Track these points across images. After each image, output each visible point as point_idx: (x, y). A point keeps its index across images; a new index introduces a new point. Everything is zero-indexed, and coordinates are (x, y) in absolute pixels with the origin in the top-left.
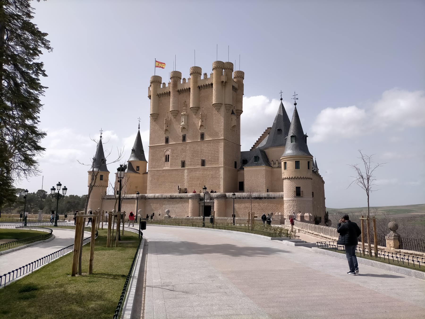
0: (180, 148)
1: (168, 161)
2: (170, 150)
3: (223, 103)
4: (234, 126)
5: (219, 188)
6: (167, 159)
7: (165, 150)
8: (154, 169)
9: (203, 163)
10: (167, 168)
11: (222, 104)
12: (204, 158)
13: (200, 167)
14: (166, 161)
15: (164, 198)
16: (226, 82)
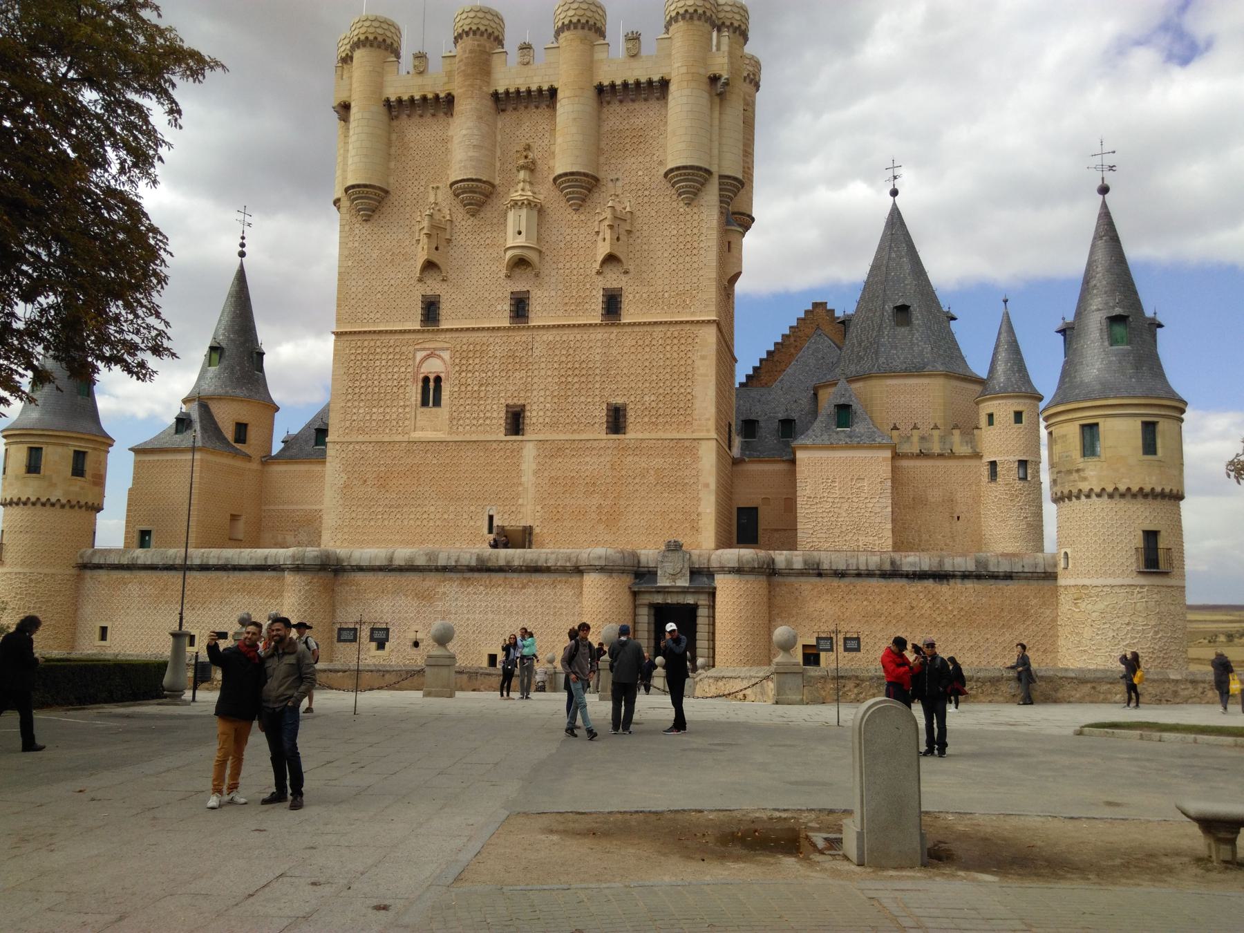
0: (498, 346)
1: (437, 403)
2: (446, 355)
3: (714, 169)
5: (695, 529)
6: (431, 391)
7: (420, 355)
8: (360, 438)
9: (616, 420)
10: (429, 435)
11: (709, 172)
12: (619, 401)
13: (604, 436)
14: (425, 403)
15: (444, 569)
16: (726, 84)
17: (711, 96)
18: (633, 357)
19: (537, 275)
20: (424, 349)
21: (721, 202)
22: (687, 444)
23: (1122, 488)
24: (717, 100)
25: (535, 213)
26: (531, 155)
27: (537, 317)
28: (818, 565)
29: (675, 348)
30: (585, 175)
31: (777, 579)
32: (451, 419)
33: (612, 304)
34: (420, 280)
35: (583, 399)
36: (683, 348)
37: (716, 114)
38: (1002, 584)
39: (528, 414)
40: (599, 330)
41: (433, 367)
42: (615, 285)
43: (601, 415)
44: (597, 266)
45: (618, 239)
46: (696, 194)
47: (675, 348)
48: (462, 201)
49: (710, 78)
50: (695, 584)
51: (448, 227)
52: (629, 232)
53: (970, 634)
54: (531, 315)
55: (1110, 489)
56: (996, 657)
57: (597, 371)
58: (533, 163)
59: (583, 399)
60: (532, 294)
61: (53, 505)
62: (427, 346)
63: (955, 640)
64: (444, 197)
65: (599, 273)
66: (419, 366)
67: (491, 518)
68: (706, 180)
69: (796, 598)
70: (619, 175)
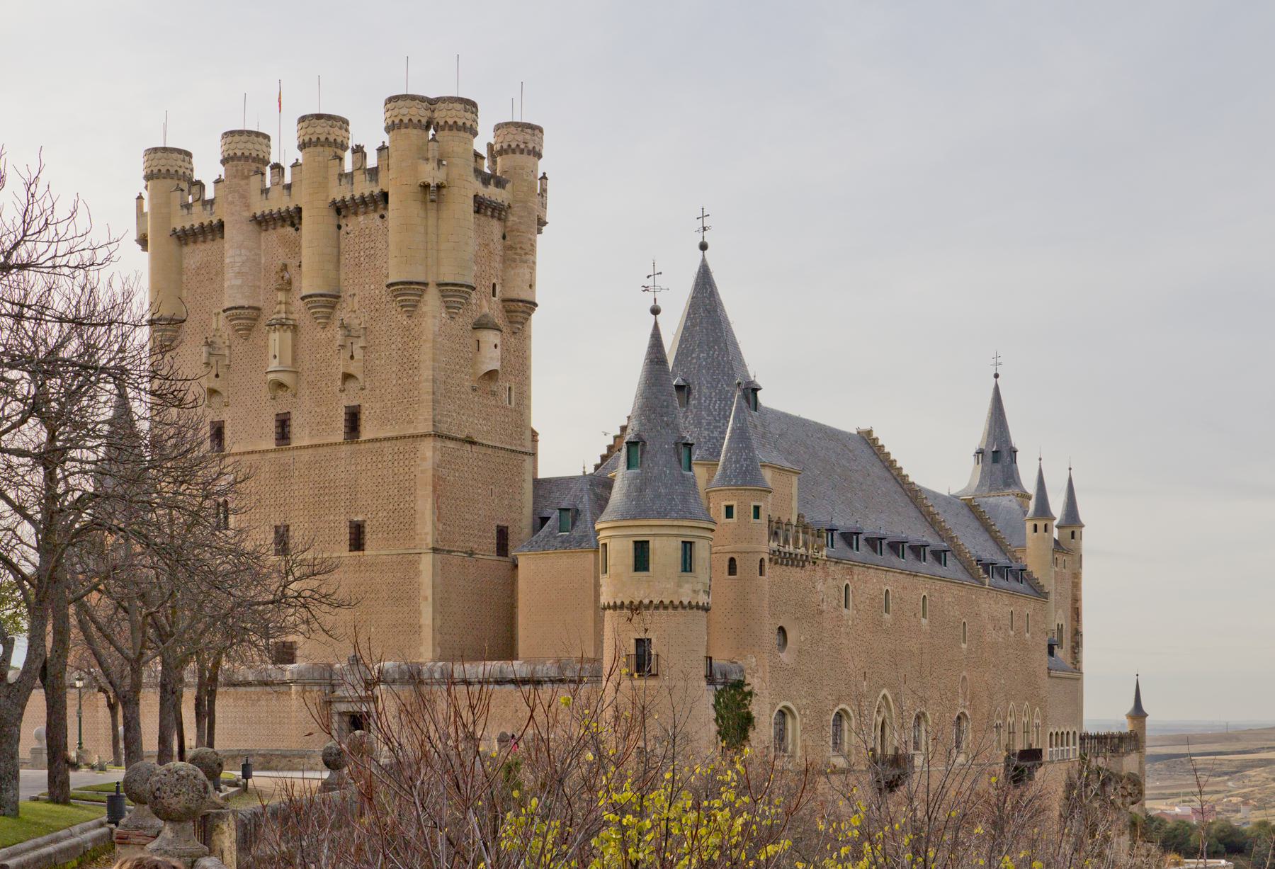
3: (430, 280)
4: (491, 375)
9: (357, 539)
11: (426, 284)
12: (359, 518)
17: (424, 202)
19: (295, 396)
22: (411, 558)
23: (619, 603)
24: (430, 205)
25: (289, 334)
26: (287, 276)
30: (321, 295)
33: (353, 420)
40: (343, 447)
42: (355, 403)
43: (345, 534)
44: (339, 383)
45: (352, 357)
46: (415, 306)
48: (234, 326)
51: (227, 352)
52: (364, 348)
54: (292, 436)
58: (289, 283)
60: (293, 415)
64: (220, 324)
65: (342, 391)
70: (356, 291)
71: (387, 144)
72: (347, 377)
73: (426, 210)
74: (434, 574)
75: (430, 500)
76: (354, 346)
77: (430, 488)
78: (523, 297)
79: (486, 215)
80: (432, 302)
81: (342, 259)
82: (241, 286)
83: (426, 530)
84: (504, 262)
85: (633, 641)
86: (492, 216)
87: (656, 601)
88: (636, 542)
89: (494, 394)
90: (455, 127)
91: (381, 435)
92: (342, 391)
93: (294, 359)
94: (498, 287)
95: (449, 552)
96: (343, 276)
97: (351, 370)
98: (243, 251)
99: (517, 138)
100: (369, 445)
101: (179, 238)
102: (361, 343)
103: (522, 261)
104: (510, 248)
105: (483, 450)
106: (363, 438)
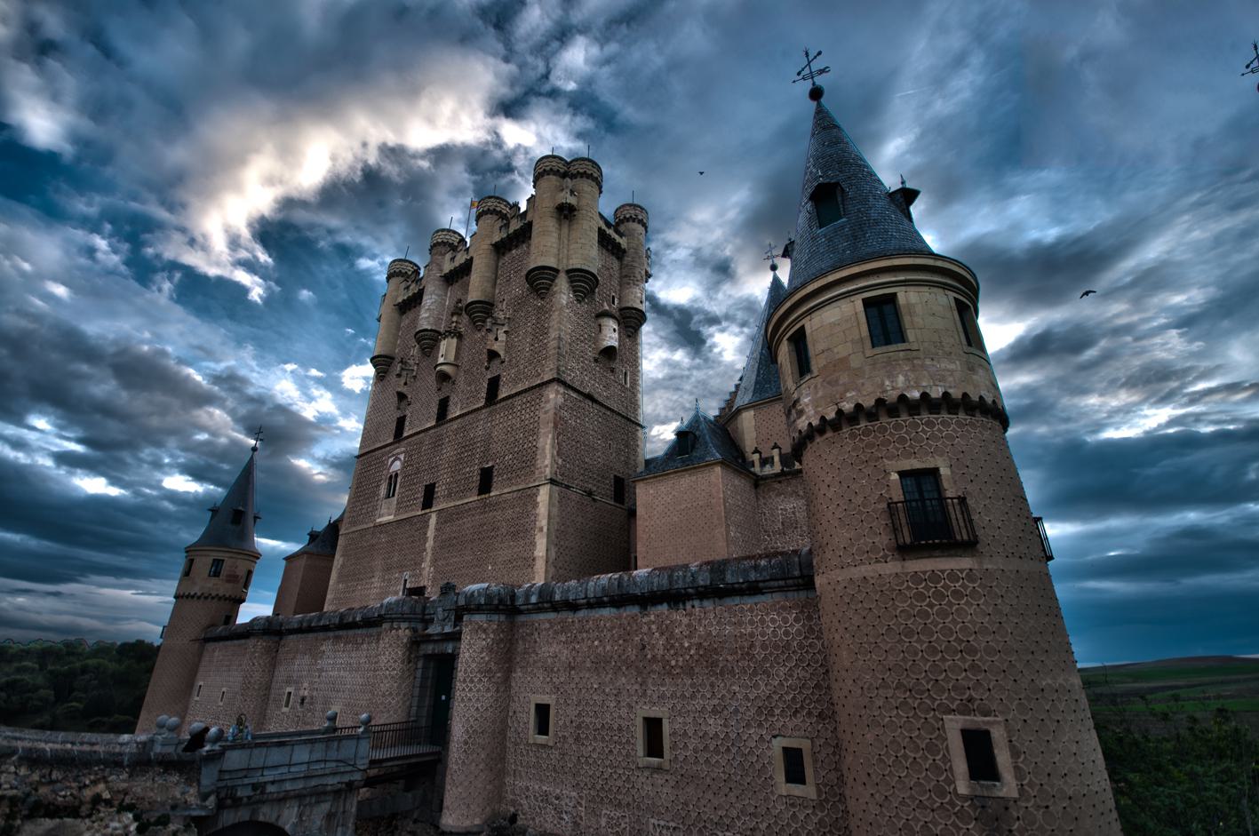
1: (393, 495)
2: (402, 457)
3: (560, 268)
4: (609, 352)
8: (354, 529)
11: (557, 271)
12: (490, 464)
14: (388, 496)
17: (559, 221)
18: (501, 425)
20: (393, 455)
21: (575, 291)
25: (455, 340)
27: (455, 411)
28: (551, 597)
29: (528, 410)
31: (522, 618)
32: (398, 503)
34: (399, 409)
35: (468, 469)
36: (533, 408)
37: (565, 230)
38: (749, 601)
39: (436, 490)
41: (397, 466)
45: (496, 339)
46: (548, 289)
47: (528, 410)
49: (557, 208)
50: (458, 628)
53: (712, 685)
55: (831, 415)
56: (748, 725)
57: (479, 445)
59: (468, 469)
60: (451, 398)
61: (193, 597)
62: (395, 452)
63: (693, 697)
66: (389, 469)
67: (406, 581)
68: (555, 277)
69: (536, 642)
71: (534, 193)
72: (493, 355)
73: (560, 225)
74: (551, 504)
75: (550, 436)
76: (499, 332)
77: (551, 425)
78: (635, 306)
79: (607, 250)
80: (562, 285)
81: (498, 281)
82: (428, 317)
83: (546, 461)
84: (621, 286)
85: (895, 476)
86: (613, 254)
87: (936, 393)
88: (866, 302)
89: (612, 371)
90: (584, 175)
91: (514, 392)
92: (487, 368)
93: (457, 357)
94: (616, 302)
95: (568, 487)
96: (497, 291)
97: (497, 347)
98: (433, 296)
99: (630, 212)
100: (502, 404)
101: (400, 309)
102: (505, 328)
103: (634, 284)
104: (626, 276)
105: (603, 410)
106: (500, 398)
